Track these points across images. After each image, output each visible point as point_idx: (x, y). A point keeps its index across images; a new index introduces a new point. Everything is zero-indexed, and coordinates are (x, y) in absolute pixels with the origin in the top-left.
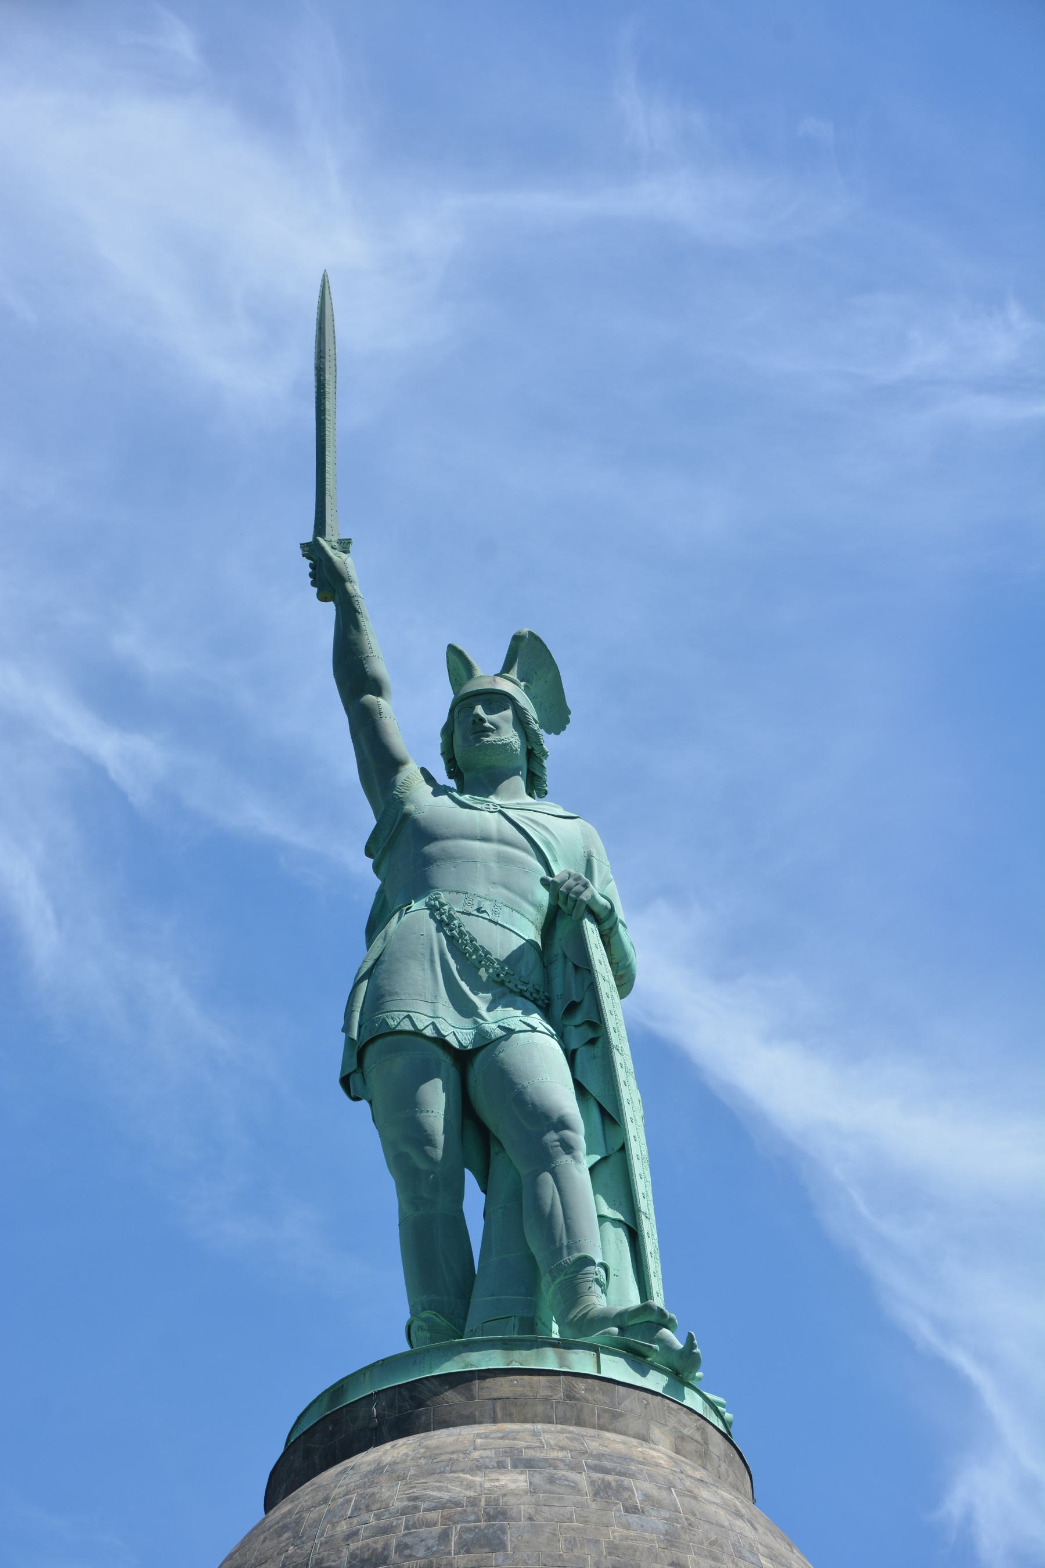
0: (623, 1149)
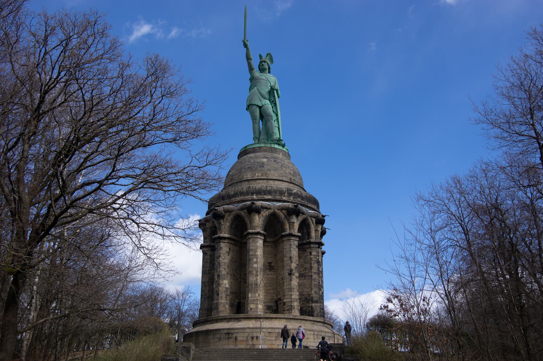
0: (278, 118)
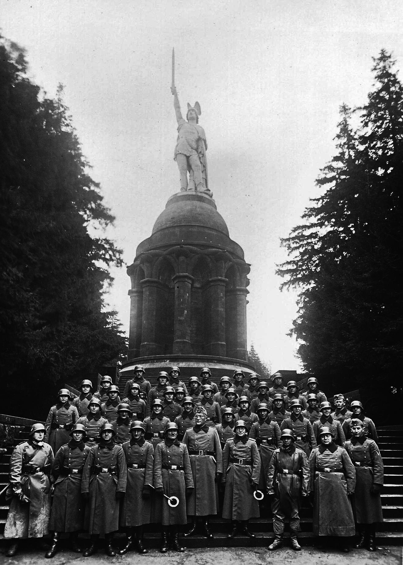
0: (205, 170)
